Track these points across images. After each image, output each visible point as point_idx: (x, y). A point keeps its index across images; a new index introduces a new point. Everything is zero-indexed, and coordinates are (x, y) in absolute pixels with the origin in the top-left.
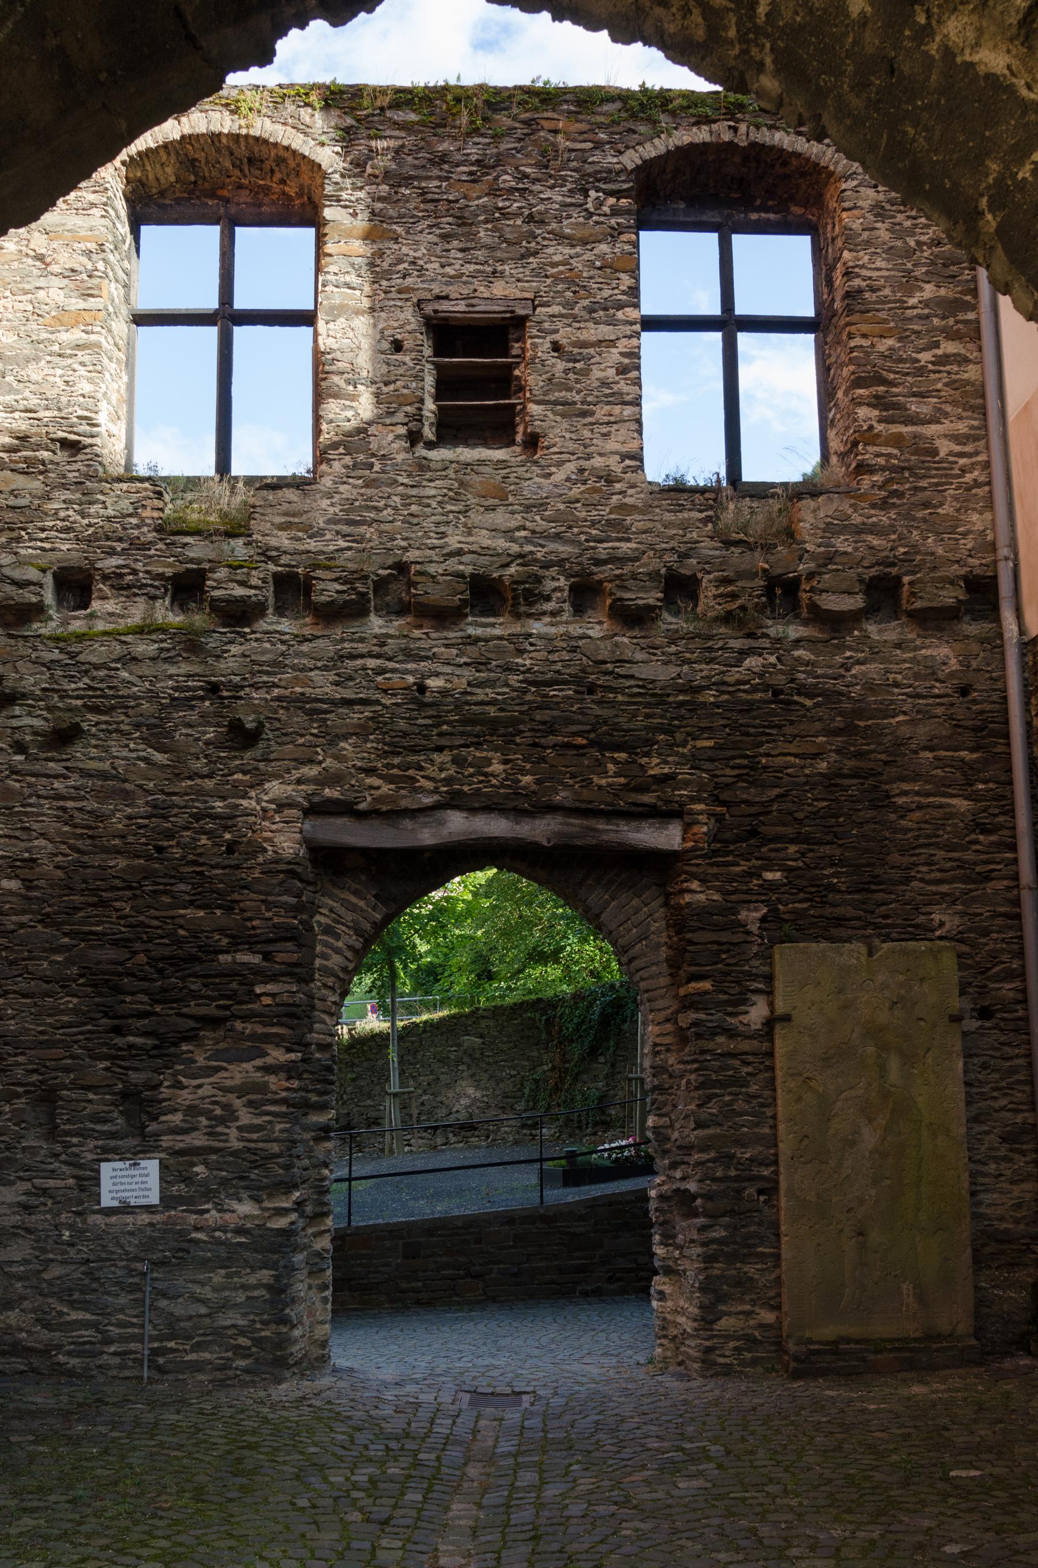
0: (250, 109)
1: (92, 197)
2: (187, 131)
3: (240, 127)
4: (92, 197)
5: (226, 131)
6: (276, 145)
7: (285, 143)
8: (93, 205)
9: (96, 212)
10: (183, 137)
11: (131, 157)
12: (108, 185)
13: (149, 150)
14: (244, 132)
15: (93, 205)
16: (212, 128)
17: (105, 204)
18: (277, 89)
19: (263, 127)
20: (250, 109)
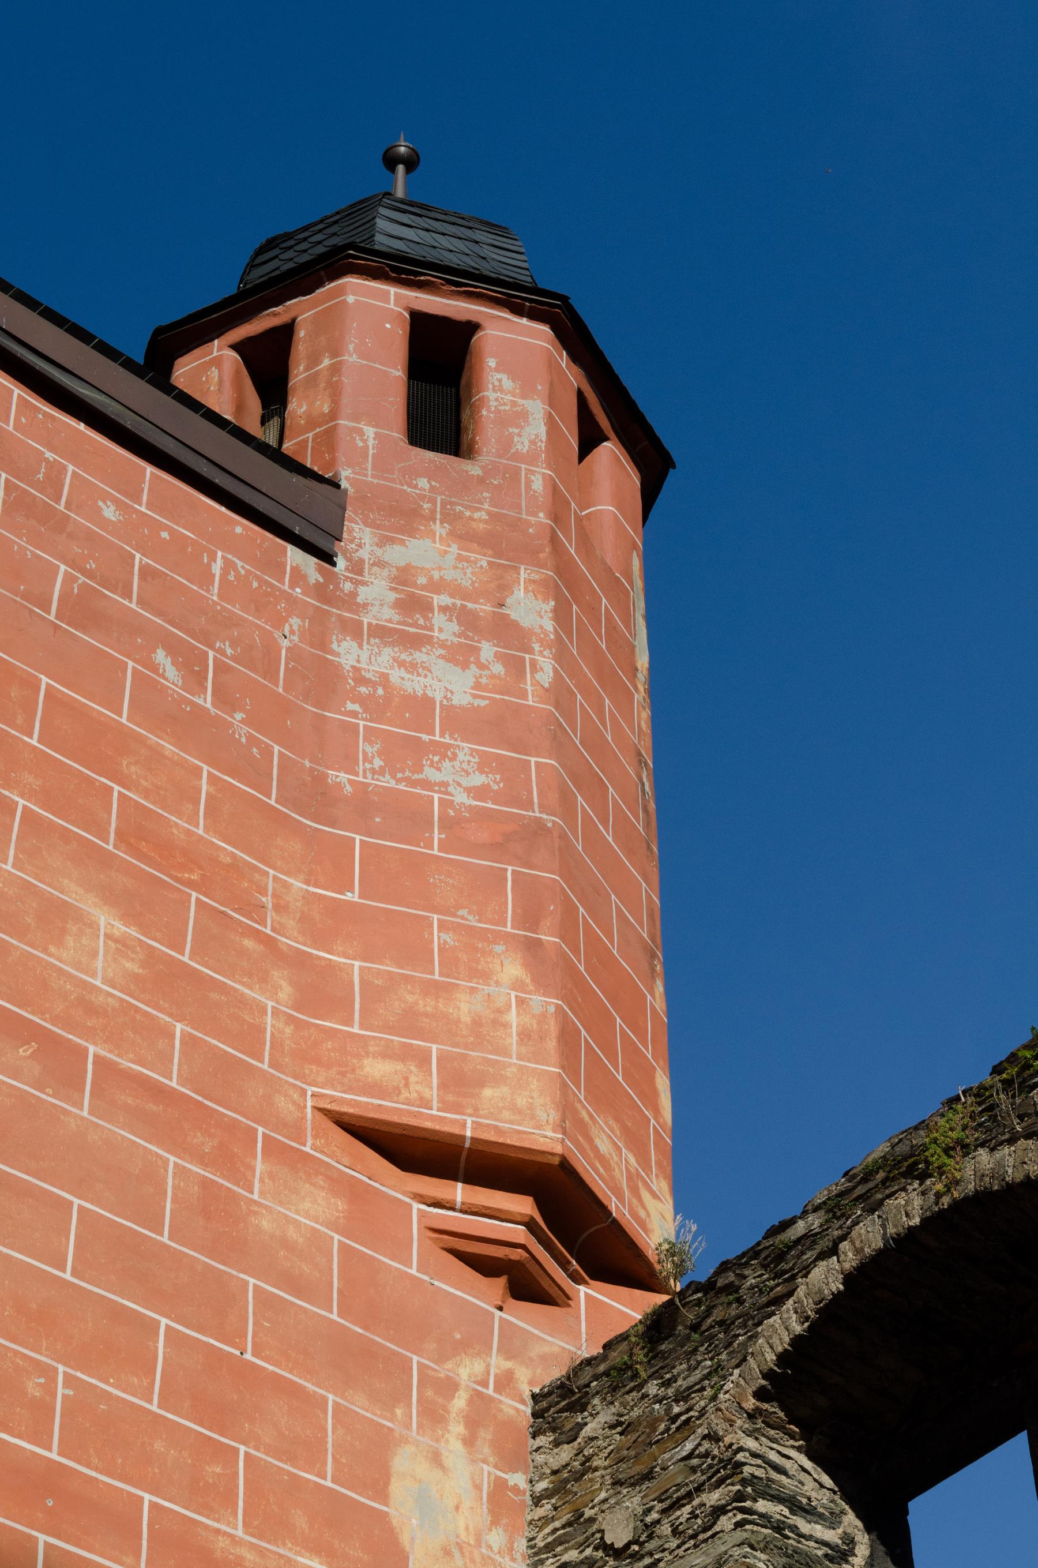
0: (947, 1151)
1: (713, 1498)
2: (849, 1257)
3: (938, 1195)
4: (713, 1498)
5: (916, 1221)
6: (1010, 1189)
7: (1019, 1177)
8: (719, 1511)
9: (725, 1522)
10: (849, 1279)
11: (768, 1375)
12: (740, 1457)
13: (797, 1341)
14: (946, 1201)
15: (719, 1511)
16: (891, 1230)
17: (740, 1497)
18: (988, 1080)
19: (984, 1167)
20: (947, 1151)
